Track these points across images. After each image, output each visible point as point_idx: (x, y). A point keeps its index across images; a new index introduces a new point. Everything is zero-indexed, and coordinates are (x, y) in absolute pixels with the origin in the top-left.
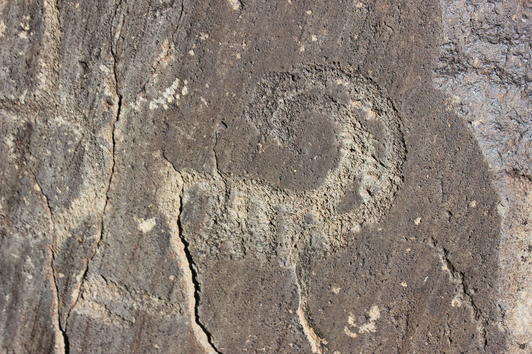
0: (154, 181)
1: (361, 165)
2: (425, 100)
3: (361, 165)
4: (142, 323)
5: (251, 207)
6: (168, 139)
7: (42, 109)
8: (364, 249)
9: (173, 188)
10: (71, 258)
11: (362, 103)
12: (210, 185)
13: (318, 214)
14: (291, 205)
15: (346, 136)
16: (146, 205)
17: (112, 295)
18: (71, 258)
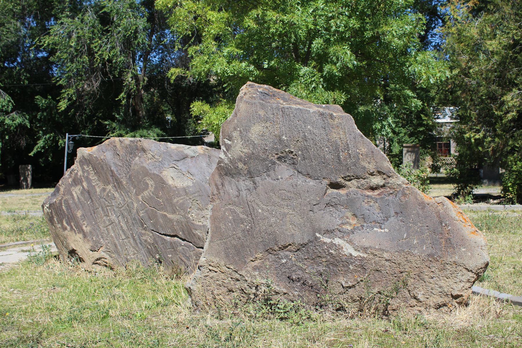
0: (138, 198)
1: (151, 183)
2: (150, 174)
3: (151, 183)
4: (146, 211)
5: (146, 193)
6: (137, 194)
7: (127, 202)
8: (156, 188)
9: (140, 197)
10: (138, 212)
11: (146, 178)
12: (142, 195)
13: (151, 189)
14: (149, 190)
15: (148, 182)
16: (139, 201)
17: (142, 212)
18: (138, 212)
